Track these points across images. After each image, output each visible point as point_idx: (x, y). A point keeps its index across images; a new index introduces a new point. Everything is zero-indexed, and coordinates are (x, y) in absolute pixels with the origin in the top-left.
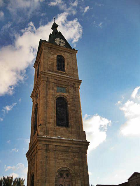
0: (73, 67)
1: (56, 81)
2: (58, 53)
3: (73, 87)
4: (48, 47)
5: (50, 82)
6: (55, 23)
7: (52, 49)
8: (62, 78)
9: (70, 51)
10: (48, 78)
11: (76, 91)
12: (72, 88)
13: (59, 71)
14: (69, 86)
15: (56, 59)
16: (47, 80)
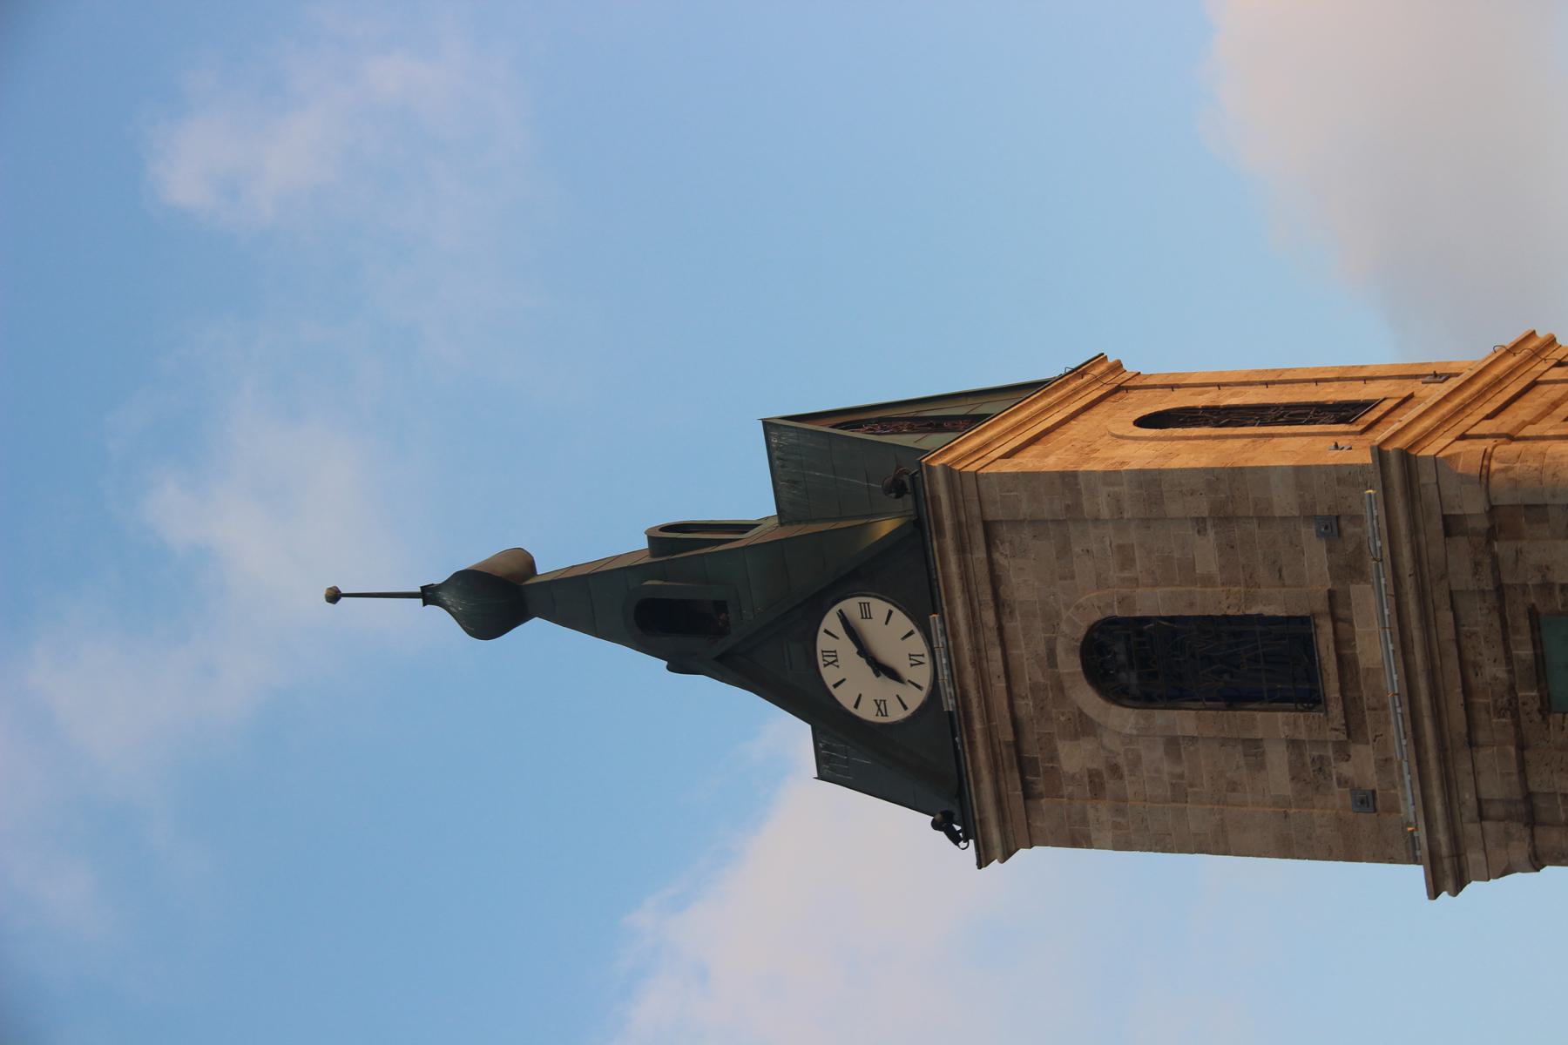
0: (1200, 523)
1: (1482, 736)
2: (1060, 689)
3: (1492, 534)
4: (1028, 794)
5: (1528, 796)
6: (429, 595)
7: (1031, 749)
8: (1432, 673)
9: (962, 549)
10: (1482, 817)
11: (1536, 511)
12: (1518, 552)
13: (1332, 687)
14: (1500, 589)
15: (1162, 718)
16: (1517, 828)
